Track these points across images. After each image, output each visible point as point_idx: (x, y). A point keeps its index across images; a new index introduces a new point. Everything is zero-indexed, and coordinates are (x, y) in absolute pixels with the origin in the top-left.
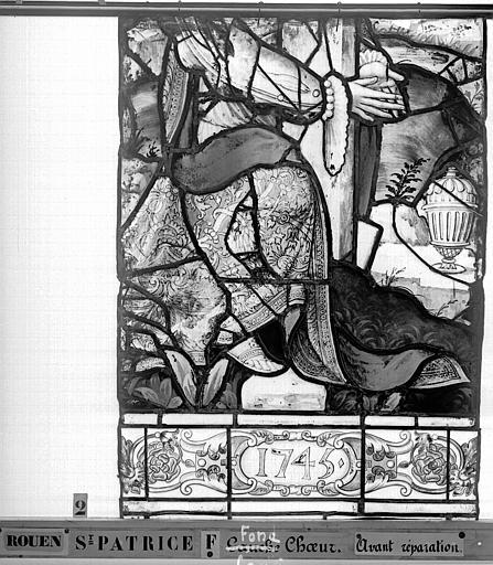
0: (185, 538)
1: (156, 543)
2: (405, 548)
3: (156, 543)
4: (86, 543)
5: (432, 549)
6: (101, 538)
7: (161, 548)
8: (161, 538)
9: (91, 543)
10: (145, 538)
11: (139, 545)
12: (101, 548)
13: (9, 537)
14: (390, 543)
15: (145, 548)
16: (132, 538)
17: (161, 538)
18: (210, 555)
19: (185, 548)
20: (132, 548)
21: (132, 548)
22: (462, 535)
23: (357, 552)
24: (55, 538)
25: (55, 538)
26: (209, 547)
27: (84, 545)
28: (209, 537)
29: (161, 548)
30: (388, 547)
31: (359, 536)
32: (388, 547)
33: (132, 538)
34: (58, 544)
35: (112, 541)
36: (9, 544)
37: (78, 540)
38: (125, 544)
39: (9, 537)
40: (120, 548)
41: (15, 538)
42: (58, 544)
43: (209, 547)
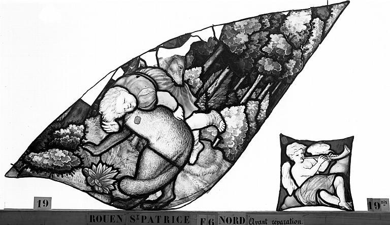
0: (186, 217)
2: (274, 222)
3: (171, 219)
4: (135, 219)
6: (143, 217)
7: (173, 222)
8: (173, 217)
9: (138, 219)
10: (165, 217)
11: (162, 220)
12: (143, 222)
14: (266, 220)
15: (165, 222)
16: (158, 217)
17: (173, 217)
19: (186, 222)
20: (158, 222)
21: (158, 222)
24: (119, 216)
25: (119, 216)
27: (134, 220)
29: (173, 222)
32: (265, 222)
33: (158, 217)
35: (148, 218)
37: (131, 217)
38: (155, 220)
40: (152, 222)
41: (101, 217)
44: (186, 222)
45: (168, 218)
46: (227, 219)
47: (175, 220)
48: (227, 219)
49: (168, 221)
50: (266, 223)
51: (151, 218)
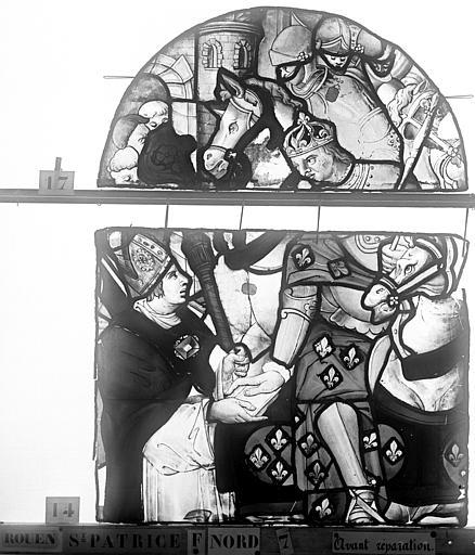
1: (145, 542)
2: (381, 547)
3: (145, 542)
5: (405, 548)
8: (150, 536)
10: (135, 536)
11: (128, 544)
13: (7, 538)
14: (366, 542)
15: (135, 546)
16: (122, 536)
17: (150, 536)
18: (196, 552)
19: (172, 546)
20: (122, 546)
21: (122, 546)
22: (433, 535)
23: (334, 551)
26: (195, 544)
28: (195, 535)
30: (363, 546)
31: (336, 535)
32: (363, 546)
34: (53, 541)
36: (7, 541)
39: (7, 535)
42: (53, 541)
43: (195, 544)
44: (172, 546)
45: (140, 537)
46: (226, 539)
47: (154, 538)
48: (226, 539)
49: (141, 544)
50: (366, 548)
51: (108, 538)
